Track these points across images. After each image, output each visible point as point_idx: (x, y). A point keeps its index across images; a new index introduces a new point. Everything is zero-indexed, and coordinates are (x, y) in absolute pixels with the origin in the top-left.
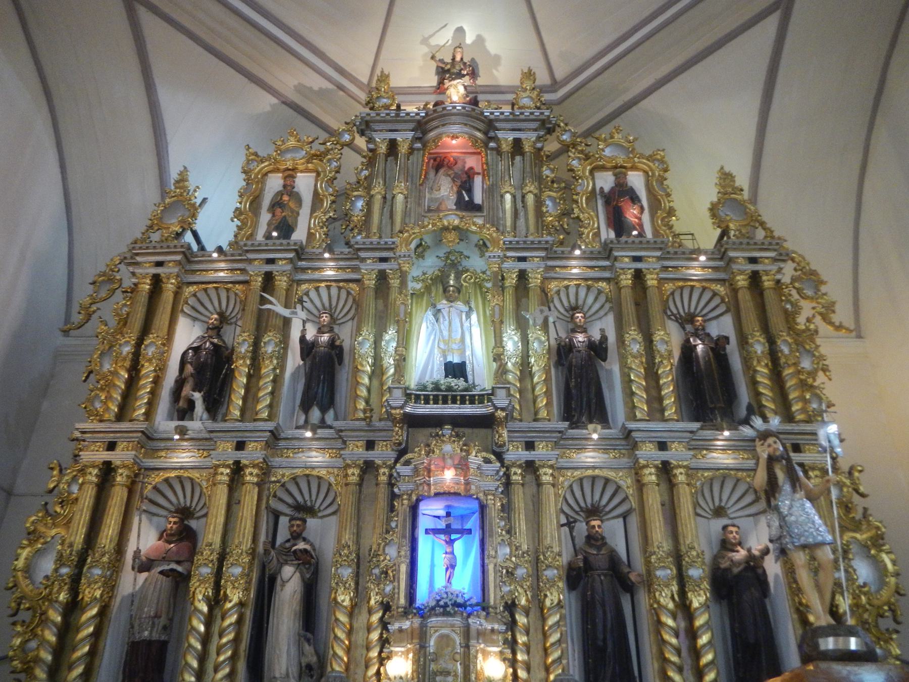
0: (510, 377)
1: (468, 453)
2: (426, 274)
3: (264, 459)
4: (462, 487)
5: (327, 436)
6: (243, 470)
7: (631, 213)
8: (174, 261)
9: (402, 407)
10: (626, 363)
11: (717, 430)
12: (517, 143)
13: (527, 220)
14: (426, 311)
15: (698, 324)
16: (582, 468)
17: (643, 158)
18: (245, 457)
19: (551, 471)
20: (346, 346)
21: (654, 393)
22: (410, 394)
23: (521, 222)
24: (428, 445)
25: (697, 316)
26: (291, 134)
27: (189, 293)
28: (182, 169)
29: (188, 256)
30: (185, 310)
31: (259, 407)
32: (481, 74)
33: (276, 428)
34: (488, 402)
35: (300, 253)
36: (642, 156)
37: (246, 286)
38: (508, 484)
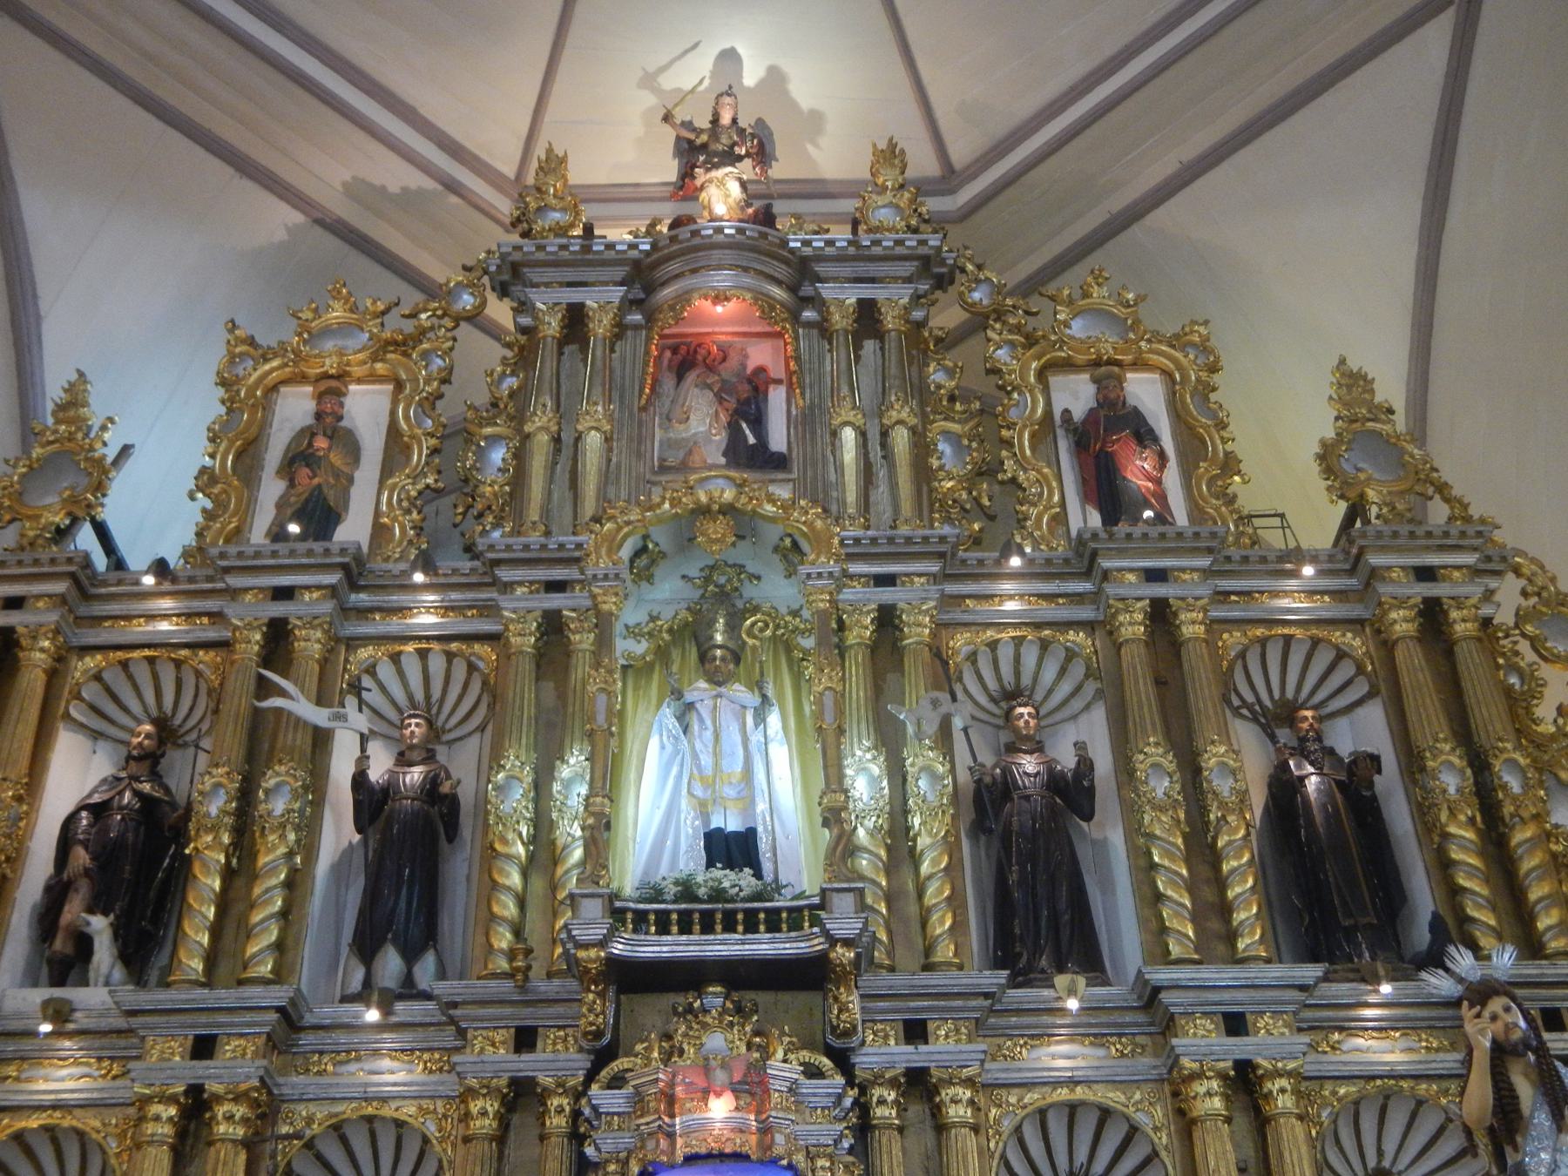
0: (864, 863)
1: (766, 1054)
2: (658, 618)
3: (262, 1079)
4: (753, 1139)
5: (418, 1019)
6: (210, 1109)
7: (1137, 469)
8: (50, 596)
9: (602, 943)
10: (1141, 823)
11: (1363, 980)
12: (867, 312)
13: (893, 486)
14: (658, 709)
15: (1305, 726)
16: (1045, 1084)
17: (1160, 342)
18: (214, 1076)
19: (968, 1094)
20: (466, 795)
21: (1209, 894)
22: (623, 911)
23: (881, 493)
24: (668, 1037)
25: (1303, 707)
26: (336, 295)
27: (85, 671)
28: (74, 377)
29: (82, 581)
30: (74, 713)
31: (252, 949)
32: (777, 153)
33: (293, 1001)
34: (811, 926)
35: (354, 572)
36: (1156, 337)
37: (223, 653)
38: (864, 1128)
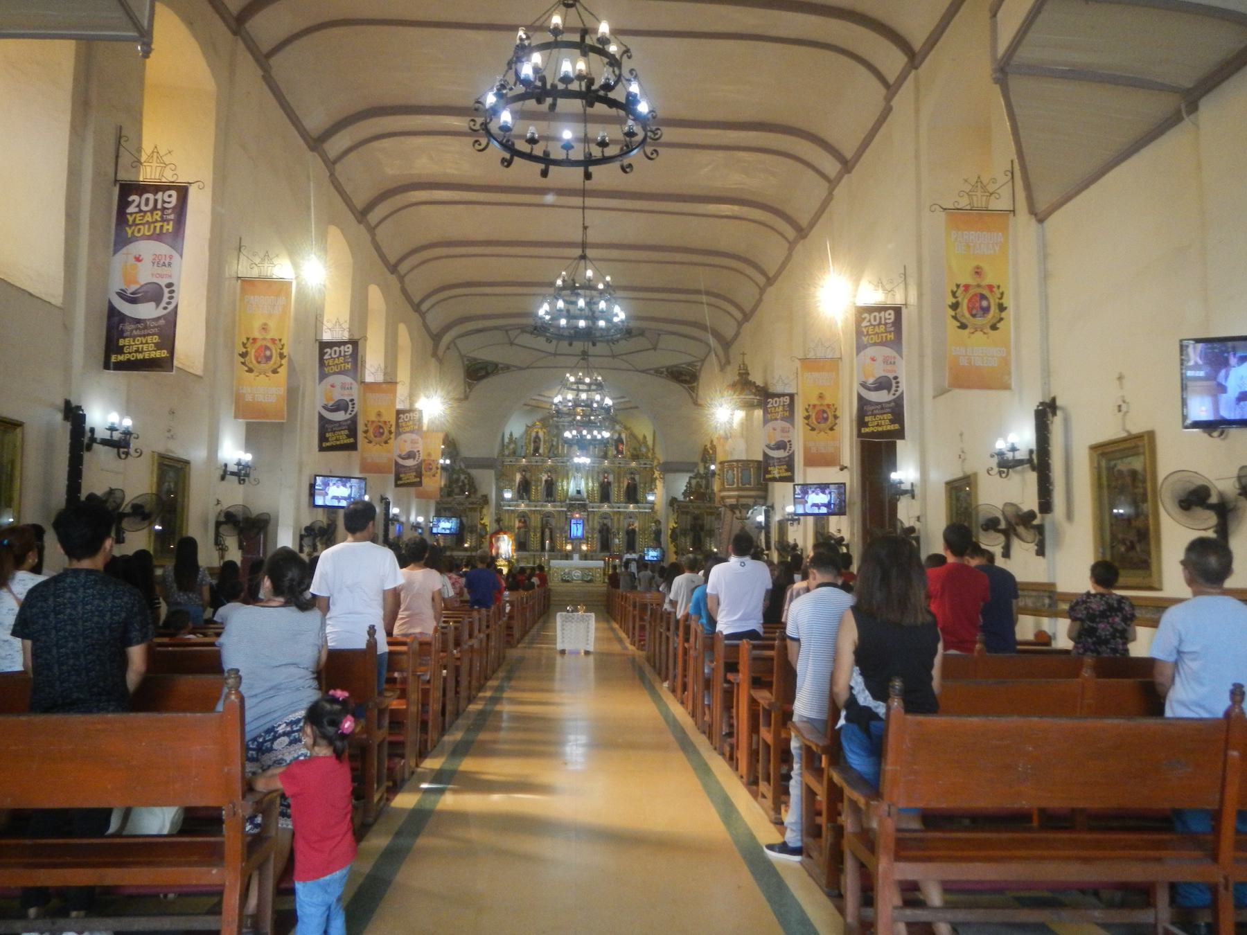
7: (621, 447)
38: (588, 515)
